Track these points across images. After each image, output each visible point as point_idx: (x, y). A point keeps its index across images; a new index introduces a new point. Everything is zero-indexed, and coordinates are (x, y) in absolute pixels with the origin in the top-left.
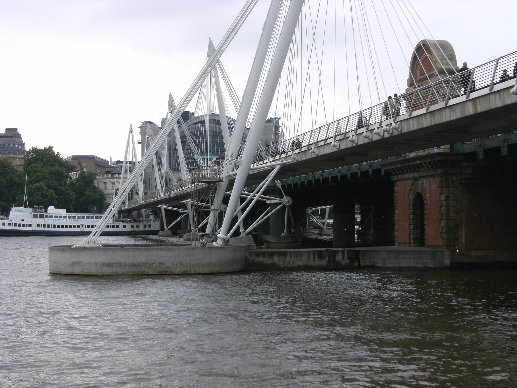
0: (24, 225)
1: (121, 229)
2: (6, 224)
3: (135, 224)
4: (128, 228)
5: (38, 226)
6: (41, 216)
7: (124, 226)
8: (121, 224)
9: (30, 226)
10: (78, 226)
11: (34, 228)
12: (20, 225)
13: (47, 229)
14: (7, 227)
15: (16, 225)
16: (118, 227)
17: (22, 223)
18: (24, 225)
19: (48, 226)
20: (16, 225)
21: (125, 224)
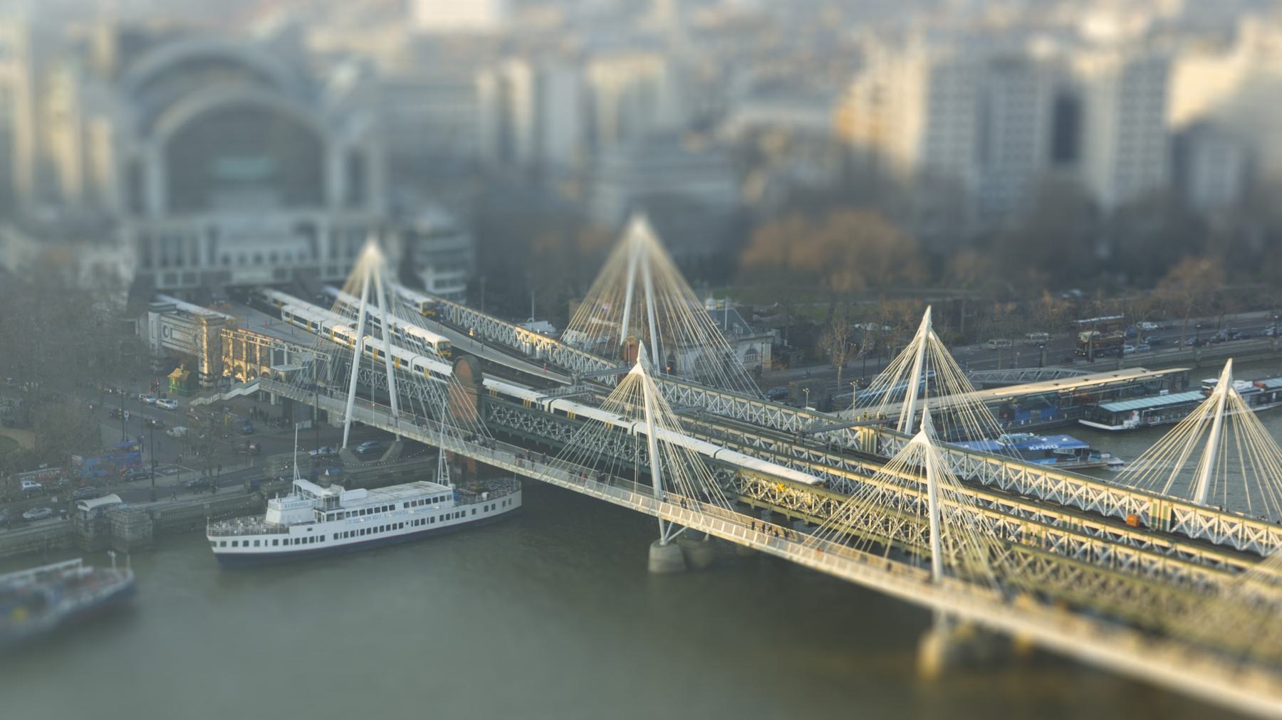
0: (312, 540)
1: (469, 518)
2: (281, 542)
3: (489, 504)
4: (481, 515)
5: (336, 536)
6: (340, 516)
7: (474, 511)
8: (468, 508)
9: (322, 538)
10: (401, 526)
11: (330, 542)
12: (305, 540)
13: (350, 540)
14: (281, 548)
15: (297, 541)
16: (464, 514)
17: (309, 535)
18: (312, 540)
19: (353, 534)
20: (297, 541)
21: (474, 506)
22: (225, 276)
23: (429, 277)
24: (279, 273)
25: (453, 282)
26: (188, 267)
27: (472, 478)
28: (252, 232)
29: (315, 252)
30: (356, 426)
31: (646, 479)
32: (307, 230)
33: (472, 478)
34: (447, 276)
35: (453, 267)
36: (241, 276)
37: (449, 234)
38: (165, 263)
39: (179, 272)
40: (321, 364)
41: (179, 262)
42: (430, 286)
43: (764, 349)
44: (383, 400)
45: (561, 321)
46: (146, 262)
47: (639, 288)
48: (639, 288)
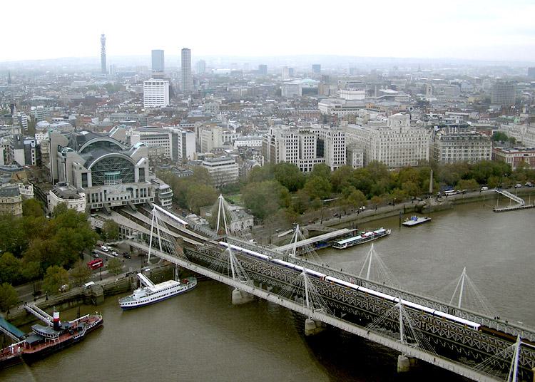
22: (110, 204)
23: (163, 201)
24: (123, 203)
25: (169, 202)
26: (99, 202)
27: (184, 275)
28: (116, 191)
29: (132, 195)
30: (152, 256)
31: (231, 275)
32: (131, 189)
33: (184, 275)
34: (167, 201)
35: (169, 198)
36: (113, 204)
37: (166, 190)
38: (93, 201)
39: (98, 203)
40: (140, 235)
41: (97, 201)
42: (163, 205)
43: (252, 220)
44: (158, 248)
45: (198, 214)
46: (89, 202)
47: (221, 210)
48: (221, 210)
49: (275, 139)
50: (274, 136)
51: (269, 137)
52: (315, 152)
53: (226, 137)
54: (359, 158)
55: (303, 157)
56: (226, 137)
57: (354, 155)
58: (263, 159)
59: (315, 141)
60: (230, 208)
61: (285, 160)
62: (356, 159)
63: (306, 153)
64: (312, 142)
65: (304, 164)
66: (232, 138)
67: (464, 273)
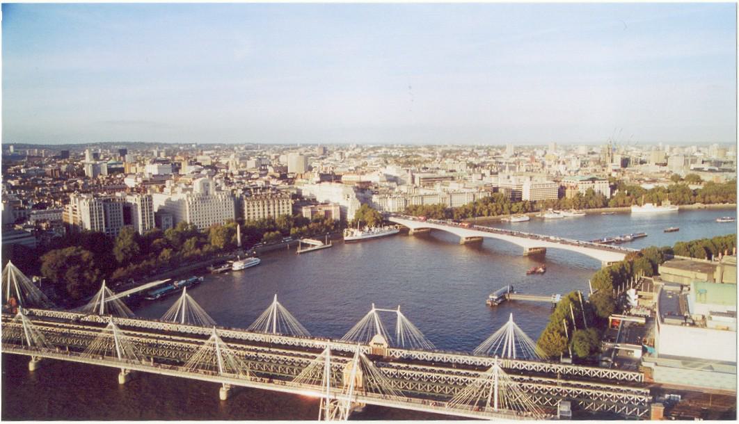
31: (25, 343)
49: (77, 209)
50: (76, 207)
51: (70, 208)
52: (122, 220)
53: (20, 213)
54: (169, 223)
55: (109, 224)
56: (20, 213)
57: (163, 220)
58: (65, 231)
59: (121, 208)
60: (25, 280)
61: (89, 229)
62: (166, 223)
63: (112, 214)
64: (118, 210)
65: (111, 232)
66: (27, 213)
67: (275, 303)
